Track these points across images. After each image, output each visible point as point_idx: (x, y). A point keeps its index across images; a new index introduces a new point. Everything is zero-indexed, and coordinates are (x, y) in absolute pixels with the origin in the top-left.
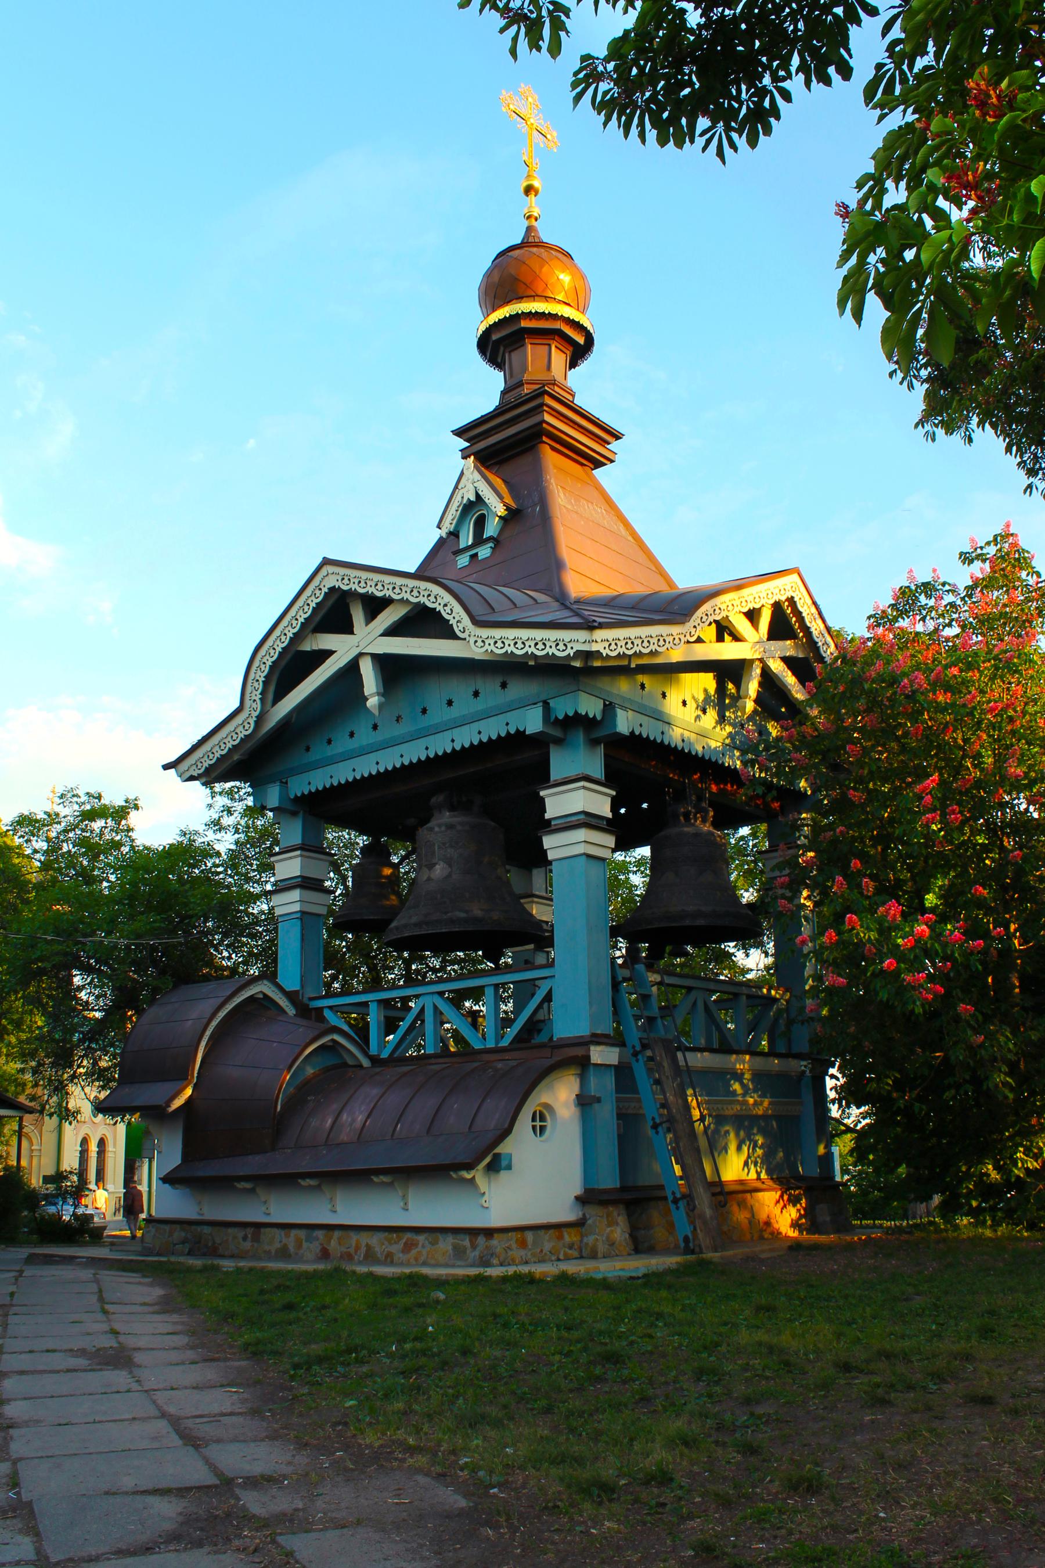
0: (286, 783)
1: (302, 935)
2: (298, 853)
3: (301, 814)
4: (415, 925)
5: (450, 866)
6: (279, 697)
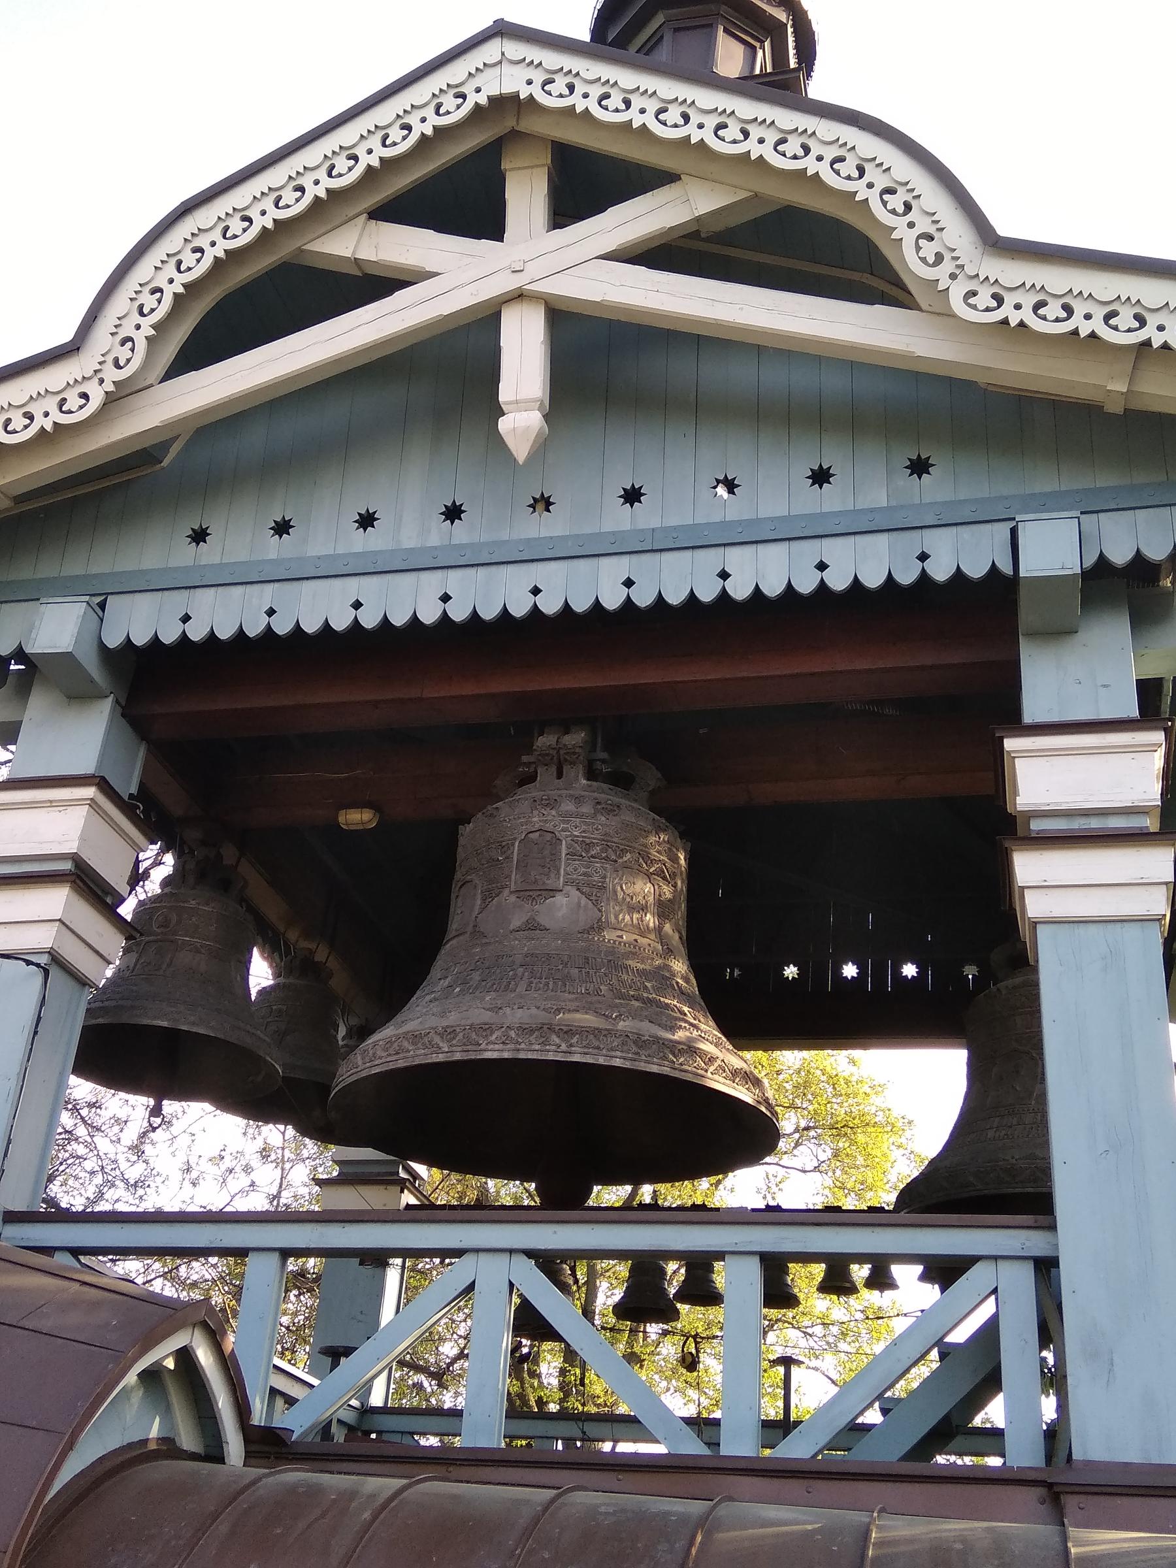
0: (102, 606)
2: (90, 792)
4: (525, 1030)
6: (197, 354)
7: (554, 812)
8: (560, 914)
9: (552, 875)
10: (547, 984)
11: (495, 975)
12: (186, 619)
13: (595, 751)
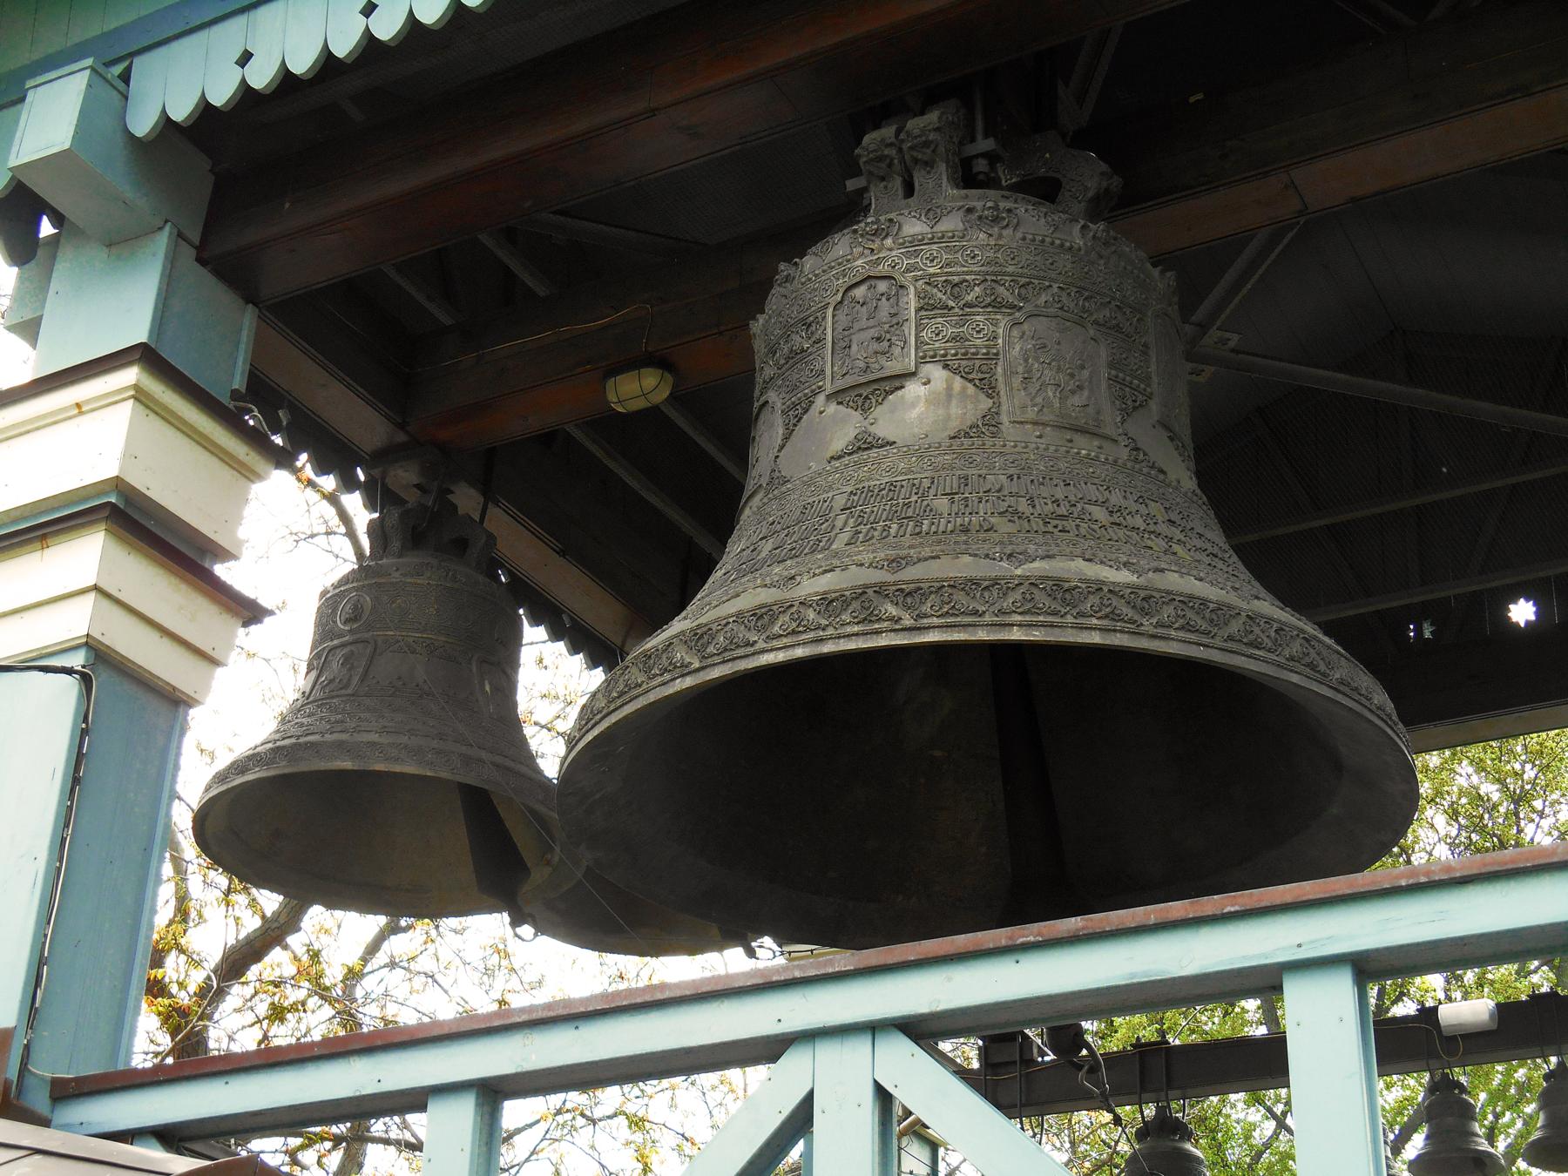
0: (126, 77)
1: (78, 759)
2: (130, 375)
3: (162, 242)
4: (829, 603)
5: (987, 387)
7: (889, 242)
8: (914, 413)
9: (897, 351)
10: (886, 528)
11: (805, 540)
12: (245, 59)
13: (973, 140)
